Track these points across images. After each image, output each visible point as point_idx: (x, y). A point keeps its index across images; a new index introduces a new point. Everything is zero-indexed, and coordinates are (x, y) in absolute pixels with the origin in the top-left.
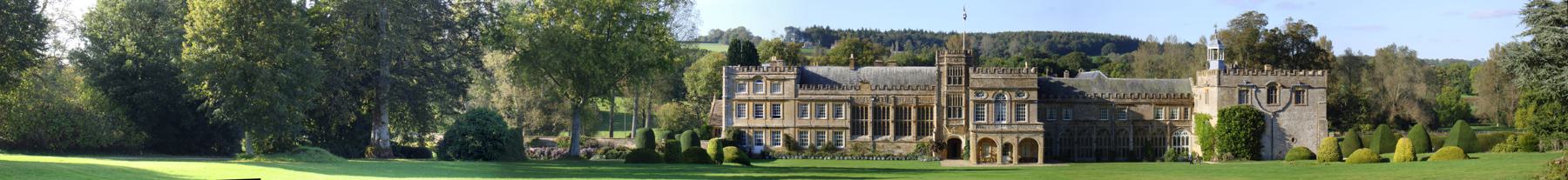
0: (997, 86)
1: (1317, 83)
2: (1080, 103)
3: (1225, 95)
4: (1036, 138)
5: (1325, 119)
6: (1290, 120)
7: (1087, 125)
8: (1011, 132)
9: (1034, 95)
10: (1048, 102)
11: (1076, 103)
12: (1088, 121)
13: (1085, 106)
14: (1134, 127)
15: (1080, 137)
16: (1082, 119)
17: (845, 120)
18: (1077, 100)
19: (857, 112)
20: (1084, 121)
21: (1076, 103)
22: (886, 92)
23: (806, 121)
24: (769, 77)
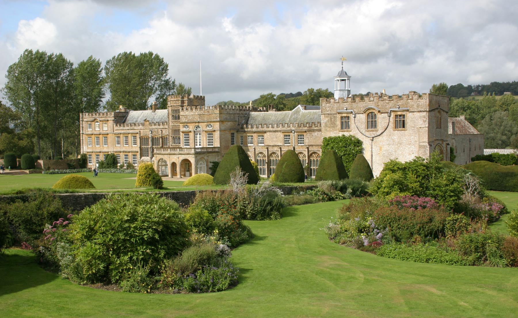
0: (195, 120)
1: (418, 106)
2: (270, 131)
3: (328, 121)
4: (190, 159)
5: (427, 144)
6: (389, 145)
8: (174, 154)
9: (217, 126)
11: (265, 132)
13: (274, 133)
15: (272, 159)
16: (272, 145)
17: (136, 148)
19: (144, 140)
20: (273, 146)
22: (157, 127)
24: (101, 119)
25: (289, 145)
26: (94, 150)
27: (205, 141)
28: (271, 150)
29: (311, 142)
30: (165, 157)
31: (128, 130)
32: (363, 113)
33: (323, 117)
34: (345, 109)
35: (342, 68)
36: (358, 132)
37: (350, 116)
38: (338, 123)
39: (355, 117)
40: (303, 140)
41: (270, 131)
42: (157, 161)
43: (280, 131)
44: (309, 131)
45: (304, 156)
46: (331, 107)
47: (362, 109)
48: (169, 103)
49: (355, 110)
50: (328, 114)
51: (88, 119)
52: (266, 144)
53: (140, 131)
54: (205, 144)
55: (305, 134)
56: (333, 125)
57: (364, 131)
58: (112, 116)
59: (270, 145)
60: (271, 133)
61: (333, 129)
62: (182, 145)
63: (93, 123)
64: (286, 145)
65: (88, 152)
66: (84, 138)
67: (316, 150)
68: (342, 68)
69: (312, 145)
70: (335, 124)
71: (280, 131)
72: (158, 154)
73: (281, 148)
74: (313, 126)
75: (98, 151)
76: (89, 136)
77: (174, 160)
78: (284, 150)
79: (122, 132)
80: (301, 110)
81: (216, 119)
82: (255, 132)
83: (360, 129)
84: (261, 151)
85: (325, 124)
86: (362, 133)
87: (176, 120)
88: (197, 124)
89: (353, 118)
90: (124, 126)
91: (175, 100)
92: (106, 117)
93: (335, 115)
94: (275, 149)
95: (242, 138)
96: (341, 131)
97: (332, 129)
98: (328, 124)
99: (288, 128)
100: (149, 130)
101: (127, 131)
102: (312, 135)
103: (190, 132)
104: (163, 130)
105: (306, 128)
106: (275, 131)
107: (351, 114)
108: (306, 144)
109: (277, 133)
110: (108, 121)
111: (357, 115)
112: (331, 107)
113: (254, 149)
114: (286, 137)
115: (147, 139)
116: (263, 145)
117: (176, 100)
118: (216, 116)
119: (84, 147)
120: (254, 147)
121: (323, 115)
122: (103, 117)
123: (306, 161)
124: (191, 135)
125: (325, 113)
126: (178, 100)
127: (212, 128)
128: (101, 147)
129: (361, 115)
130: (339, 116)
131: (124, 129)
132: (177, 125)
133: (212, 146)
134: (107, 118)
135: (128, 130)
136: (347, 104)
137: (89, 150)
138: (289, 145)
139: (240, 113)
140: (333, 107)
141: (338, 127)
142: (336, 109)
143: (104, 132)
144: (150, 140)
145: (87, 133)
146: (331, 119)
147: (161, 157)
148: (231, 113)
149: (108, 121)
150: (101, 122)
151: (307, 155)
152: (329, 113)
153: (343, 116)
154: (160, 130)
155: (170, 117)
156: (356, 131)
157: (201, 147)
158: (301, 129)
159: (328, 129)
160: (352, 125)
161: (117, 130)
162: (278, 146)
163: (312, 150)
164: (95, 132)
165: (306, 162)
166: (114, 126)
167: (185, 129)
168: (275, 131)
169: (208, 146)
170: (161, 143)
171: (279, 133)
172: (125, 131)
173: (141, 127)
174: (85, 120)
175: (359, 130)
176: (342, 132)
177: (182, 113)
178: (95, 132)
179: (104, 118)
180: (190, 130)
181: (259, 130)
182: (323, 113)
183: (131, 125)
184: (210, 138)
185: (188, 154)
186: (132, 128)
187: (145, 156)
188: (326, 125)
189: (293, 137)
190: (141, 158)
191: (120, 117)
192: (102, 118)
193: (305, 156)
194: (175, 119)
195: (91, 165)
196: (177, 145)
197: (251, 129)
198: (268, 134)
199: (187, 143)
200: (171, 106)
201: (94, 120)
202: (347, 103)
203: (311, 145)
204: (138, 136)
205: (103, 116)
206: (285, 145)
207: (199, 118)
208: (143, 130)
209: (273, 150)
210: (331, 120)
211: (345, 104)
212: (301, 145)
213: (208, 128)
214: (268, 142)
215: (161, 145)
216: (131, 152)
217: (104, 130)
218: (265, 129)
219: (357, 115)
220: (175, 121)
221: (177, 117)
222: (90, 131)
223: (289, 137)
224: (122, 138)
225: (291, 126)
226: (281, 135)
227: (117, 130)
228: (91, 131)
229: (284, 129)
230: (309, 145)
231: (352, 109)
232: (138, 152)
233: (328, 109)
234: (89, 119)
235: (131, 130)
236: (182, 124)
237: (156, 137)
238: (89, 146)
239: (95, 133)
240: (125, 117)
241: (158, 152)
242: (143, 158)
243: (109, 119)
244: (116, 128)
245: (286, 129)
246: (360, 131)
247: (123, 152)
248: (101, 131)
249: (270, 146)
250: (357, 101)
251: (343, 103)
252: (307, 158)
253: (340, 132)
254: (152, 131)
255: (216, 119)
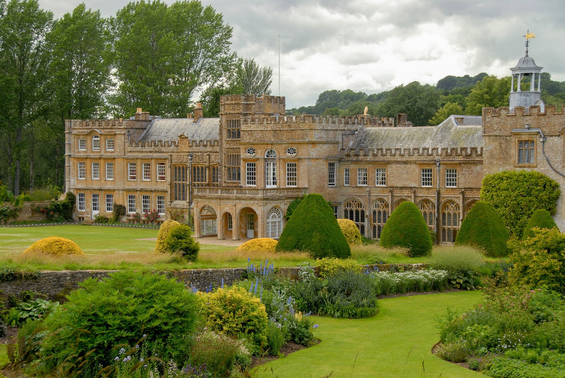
2: (397, 162)
4: (254, 208)
7: (406, 193)
8: (228, 199)
10: (357, 162)
11: (389, 163)
12: (407, 188)
13: (403, 166)
14: (464, 199)
16: (399, 185)
17: (165, 185)
18: (392, 159)
20: (402, 188)
21: (389, 163)
22: (202, 148)
23: (143, 183)
25: (430, 186)
26: (90, 186)
27: (282, 176)
28: (397, 193)
29: (469, 183)
30: (213, 204)
31: (151, 152)
32: (559, 136)
33: (487, 140)
34: (526, 127)
35: (527, 52)
36: (550, 169)
37: (534, 139)
38: (514, 152)
39: (543, 142)
40: (454, 178)
41: (397, 162)
42: (198, 210)
43: (415, 162)
44: (466, 163)
45: (457, 206)
46: (502, 124)
47: (557, 127)
48: (222, 108)
49: (544, 129)
50: (496, 136)
51: (79, 130)
52: (390, 184)
53: (171, 155)
54: (282, 181)
55: (458, 169)
56: (504, 156)
57: (560, 167)
58: (122, 127)
59: (397, 185)
60: (398, 165)
61: (503, 163)
62: (243, 182)
63: (89, 137)
64: (425, 186)
65: (78, 189)
66: (71, 165)
67: (477, 196)
68: (527, 52)
69: (472, 188)
70: (507, 153)
71: (415, 162)
72: (201, 197)
73: (415, 193)
74: (474, 155)
75: (96, 187)
76: (82, 160)
77: (227, 209)
78: (421, 195)
79: (140, 155)
80: (453, 125)
81: (303, 138)
82: (370, 162)
83: (552, 164)
84: (381, 195)
85: (489, 153)
86: (556, 171)
87: (234, 139)
88: (270, 147)
89: (541, 144)
90: (143, 146)
91: (232, 104)
92: (112, 129)
93: (508, 138)
94: (406, 193)
95: (347, 173)
96: (518, 167)
97: (501, 163)
98: (495, 152)
99: (429, 157)
100: (186, 154)
101: (149, 154)
102: (472, 171)
103: (257, 159)
104: (211, 154)
105: (461, 158)
106: (406, 163)
107: (538, 137)
108: (461, 186)
109: (409, 165)
110: (115, 135)
111: (549, 139)
112: (502, 124)
113: (367, 193)
114: (425, 173)
115: (184, 169)
116: (384, 186)
117: (235, 104)
118: (303, 134)
119: (72, 180)
120: (368, 189)
121: (487, 138)
122: (107, 128)
123: (459, 215)
124: (260, 166)
125: (491, 134)
126: (238, 104)
127: (294, 154)
128: (103, 182)
129: (556, 139)
130: (515, 140)
131: (144, 150)
132: (235, 147)
133: (294, 186)
134: (114, 130)
135: (151, 152)
136: (530, 119)
137: (79, 186)
138: (430, 186)
139: (346, 129)
140: (504, 123)
141: (512, 160)
142: (509, 126)
143: (108, 154)
144: (188, 171)
145: (77, 155)
146: (501, 144)
147: (207, 203)
148: (329, 128)
149: (115, 135)
150: (103, 137)
151: (461, 205)
152: (497, 134)
153: (522, 139)
154: (206, 154)
155: (225, 132)
156: (545, 167)
157: (275, 186)
158: (451, 159)
159: (495, 162)
160: (538, 155)
161: (131, 152)
162: (411, 188)
163: (471, 196)
164: (91, 154)
165: (459, 217)
166: (127, 144)
167: (249, 154)
168: (406, 163)
169: (287, 186)
170: (207, 177)
171: (413, 166)
172: (145, 154)
173: (173, 147)
174: (74, 132)
175: (550, 165)
176: (520, 167)
177: (243, 127)
178: (91, 154)
179: (108, 130)
180: (258, 156)
181: (377, 159)
182: (486, 134)
183: (155, 144)
184: (292, 172)
185: (252, 199)
186: (157, 150)
187: (180, 199)
188: (492, 156)
189: (439, 174)
190: (171, 202)
191: (137, 129)
192: (105, 130)
193: (459, 207)
194: (233, 138)
195: (83, 213)
196: (235, 183)
197: (363, 157)
198: (394, 166)
199: (252, 179)
200: (226, 114)
201: (91, 133)
202: (531, 117)
203: (469, 188)
204: (168, 164)
205: (106, 127)
206: (423, 186)
207: (274, 136)
208: (177, 154)
209: (400, 195)
210: (501, 146)
211: (527, 118)
212: (452, 187)
213: (289, 154)
214: (392, 182)
215: (207, 181)
216: (155, 191)
217: (107, 152)
218: (388, 158)
219: (549, 139)
220: (233, 141)
221: (235, 134)
222: (82, 152)
223: (430, 173)
224: (140, 168)
225: (435, 154)
226: (416, 170)
227: (131, 152)
228: (85, 152)
229: (422, 158)
230: (464, 188)
231: (538, 128)
232: (166, 192)
233: (495, 127)
234: (81, 131)
235: (156, 152)
236: (245, 146)
237: (200, 166)
238: (81, 179)
239: (92, 155)
240: (145, 129)
241: (200, 194)
242: (176, 202)
243: (117, 132)
244: (129, 149)
245: (424, 159)
246: (552, 168)
247: (141, 190)
248: (103, 153)
249: (397, 187)
250: (548, 114)
251: (525, 117)
252: (461, 211)
253: (515, 167)
254: (192, 156)
255: (303, 138)
